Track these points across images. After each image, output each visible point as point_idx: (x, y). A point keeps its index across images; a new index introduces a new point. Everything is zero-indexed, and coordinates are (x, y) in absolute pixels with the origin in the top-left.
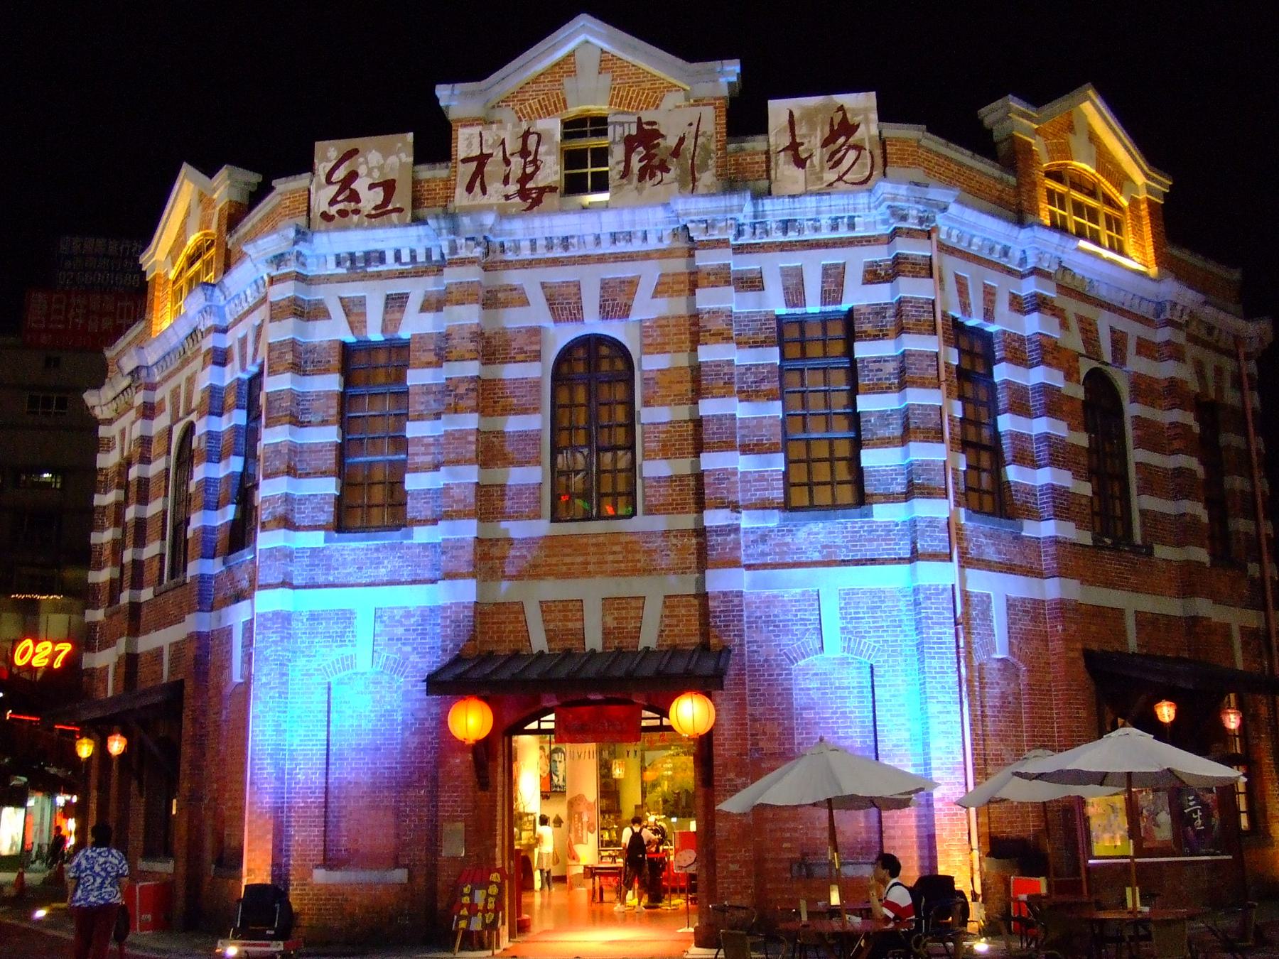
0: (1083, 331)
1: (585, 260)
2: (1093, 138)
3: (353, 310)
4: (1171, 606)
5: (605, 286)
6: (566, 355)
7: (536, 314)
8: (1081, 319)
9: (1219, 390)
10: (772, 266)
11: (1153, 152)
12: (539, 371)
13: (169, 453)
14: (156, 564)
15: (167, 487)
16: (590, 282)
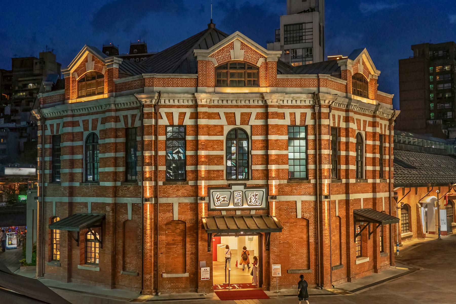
0: (357, 123)
1: (237, 107)
2: (364, 63)
3: (170, 116)
4: (370, 195)
5: (242, 114)
6: (229, 133)
7: (223, 121)
8: (357, 119)
9: (385, 131)
10: (287, 112)
11: (377, 66)
12: (223, 138)
13: (82, 140)
14: (80, 175)
15: (82, 151)
16: (238, 112)
